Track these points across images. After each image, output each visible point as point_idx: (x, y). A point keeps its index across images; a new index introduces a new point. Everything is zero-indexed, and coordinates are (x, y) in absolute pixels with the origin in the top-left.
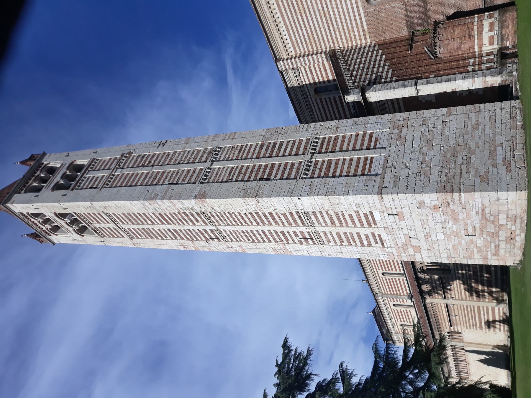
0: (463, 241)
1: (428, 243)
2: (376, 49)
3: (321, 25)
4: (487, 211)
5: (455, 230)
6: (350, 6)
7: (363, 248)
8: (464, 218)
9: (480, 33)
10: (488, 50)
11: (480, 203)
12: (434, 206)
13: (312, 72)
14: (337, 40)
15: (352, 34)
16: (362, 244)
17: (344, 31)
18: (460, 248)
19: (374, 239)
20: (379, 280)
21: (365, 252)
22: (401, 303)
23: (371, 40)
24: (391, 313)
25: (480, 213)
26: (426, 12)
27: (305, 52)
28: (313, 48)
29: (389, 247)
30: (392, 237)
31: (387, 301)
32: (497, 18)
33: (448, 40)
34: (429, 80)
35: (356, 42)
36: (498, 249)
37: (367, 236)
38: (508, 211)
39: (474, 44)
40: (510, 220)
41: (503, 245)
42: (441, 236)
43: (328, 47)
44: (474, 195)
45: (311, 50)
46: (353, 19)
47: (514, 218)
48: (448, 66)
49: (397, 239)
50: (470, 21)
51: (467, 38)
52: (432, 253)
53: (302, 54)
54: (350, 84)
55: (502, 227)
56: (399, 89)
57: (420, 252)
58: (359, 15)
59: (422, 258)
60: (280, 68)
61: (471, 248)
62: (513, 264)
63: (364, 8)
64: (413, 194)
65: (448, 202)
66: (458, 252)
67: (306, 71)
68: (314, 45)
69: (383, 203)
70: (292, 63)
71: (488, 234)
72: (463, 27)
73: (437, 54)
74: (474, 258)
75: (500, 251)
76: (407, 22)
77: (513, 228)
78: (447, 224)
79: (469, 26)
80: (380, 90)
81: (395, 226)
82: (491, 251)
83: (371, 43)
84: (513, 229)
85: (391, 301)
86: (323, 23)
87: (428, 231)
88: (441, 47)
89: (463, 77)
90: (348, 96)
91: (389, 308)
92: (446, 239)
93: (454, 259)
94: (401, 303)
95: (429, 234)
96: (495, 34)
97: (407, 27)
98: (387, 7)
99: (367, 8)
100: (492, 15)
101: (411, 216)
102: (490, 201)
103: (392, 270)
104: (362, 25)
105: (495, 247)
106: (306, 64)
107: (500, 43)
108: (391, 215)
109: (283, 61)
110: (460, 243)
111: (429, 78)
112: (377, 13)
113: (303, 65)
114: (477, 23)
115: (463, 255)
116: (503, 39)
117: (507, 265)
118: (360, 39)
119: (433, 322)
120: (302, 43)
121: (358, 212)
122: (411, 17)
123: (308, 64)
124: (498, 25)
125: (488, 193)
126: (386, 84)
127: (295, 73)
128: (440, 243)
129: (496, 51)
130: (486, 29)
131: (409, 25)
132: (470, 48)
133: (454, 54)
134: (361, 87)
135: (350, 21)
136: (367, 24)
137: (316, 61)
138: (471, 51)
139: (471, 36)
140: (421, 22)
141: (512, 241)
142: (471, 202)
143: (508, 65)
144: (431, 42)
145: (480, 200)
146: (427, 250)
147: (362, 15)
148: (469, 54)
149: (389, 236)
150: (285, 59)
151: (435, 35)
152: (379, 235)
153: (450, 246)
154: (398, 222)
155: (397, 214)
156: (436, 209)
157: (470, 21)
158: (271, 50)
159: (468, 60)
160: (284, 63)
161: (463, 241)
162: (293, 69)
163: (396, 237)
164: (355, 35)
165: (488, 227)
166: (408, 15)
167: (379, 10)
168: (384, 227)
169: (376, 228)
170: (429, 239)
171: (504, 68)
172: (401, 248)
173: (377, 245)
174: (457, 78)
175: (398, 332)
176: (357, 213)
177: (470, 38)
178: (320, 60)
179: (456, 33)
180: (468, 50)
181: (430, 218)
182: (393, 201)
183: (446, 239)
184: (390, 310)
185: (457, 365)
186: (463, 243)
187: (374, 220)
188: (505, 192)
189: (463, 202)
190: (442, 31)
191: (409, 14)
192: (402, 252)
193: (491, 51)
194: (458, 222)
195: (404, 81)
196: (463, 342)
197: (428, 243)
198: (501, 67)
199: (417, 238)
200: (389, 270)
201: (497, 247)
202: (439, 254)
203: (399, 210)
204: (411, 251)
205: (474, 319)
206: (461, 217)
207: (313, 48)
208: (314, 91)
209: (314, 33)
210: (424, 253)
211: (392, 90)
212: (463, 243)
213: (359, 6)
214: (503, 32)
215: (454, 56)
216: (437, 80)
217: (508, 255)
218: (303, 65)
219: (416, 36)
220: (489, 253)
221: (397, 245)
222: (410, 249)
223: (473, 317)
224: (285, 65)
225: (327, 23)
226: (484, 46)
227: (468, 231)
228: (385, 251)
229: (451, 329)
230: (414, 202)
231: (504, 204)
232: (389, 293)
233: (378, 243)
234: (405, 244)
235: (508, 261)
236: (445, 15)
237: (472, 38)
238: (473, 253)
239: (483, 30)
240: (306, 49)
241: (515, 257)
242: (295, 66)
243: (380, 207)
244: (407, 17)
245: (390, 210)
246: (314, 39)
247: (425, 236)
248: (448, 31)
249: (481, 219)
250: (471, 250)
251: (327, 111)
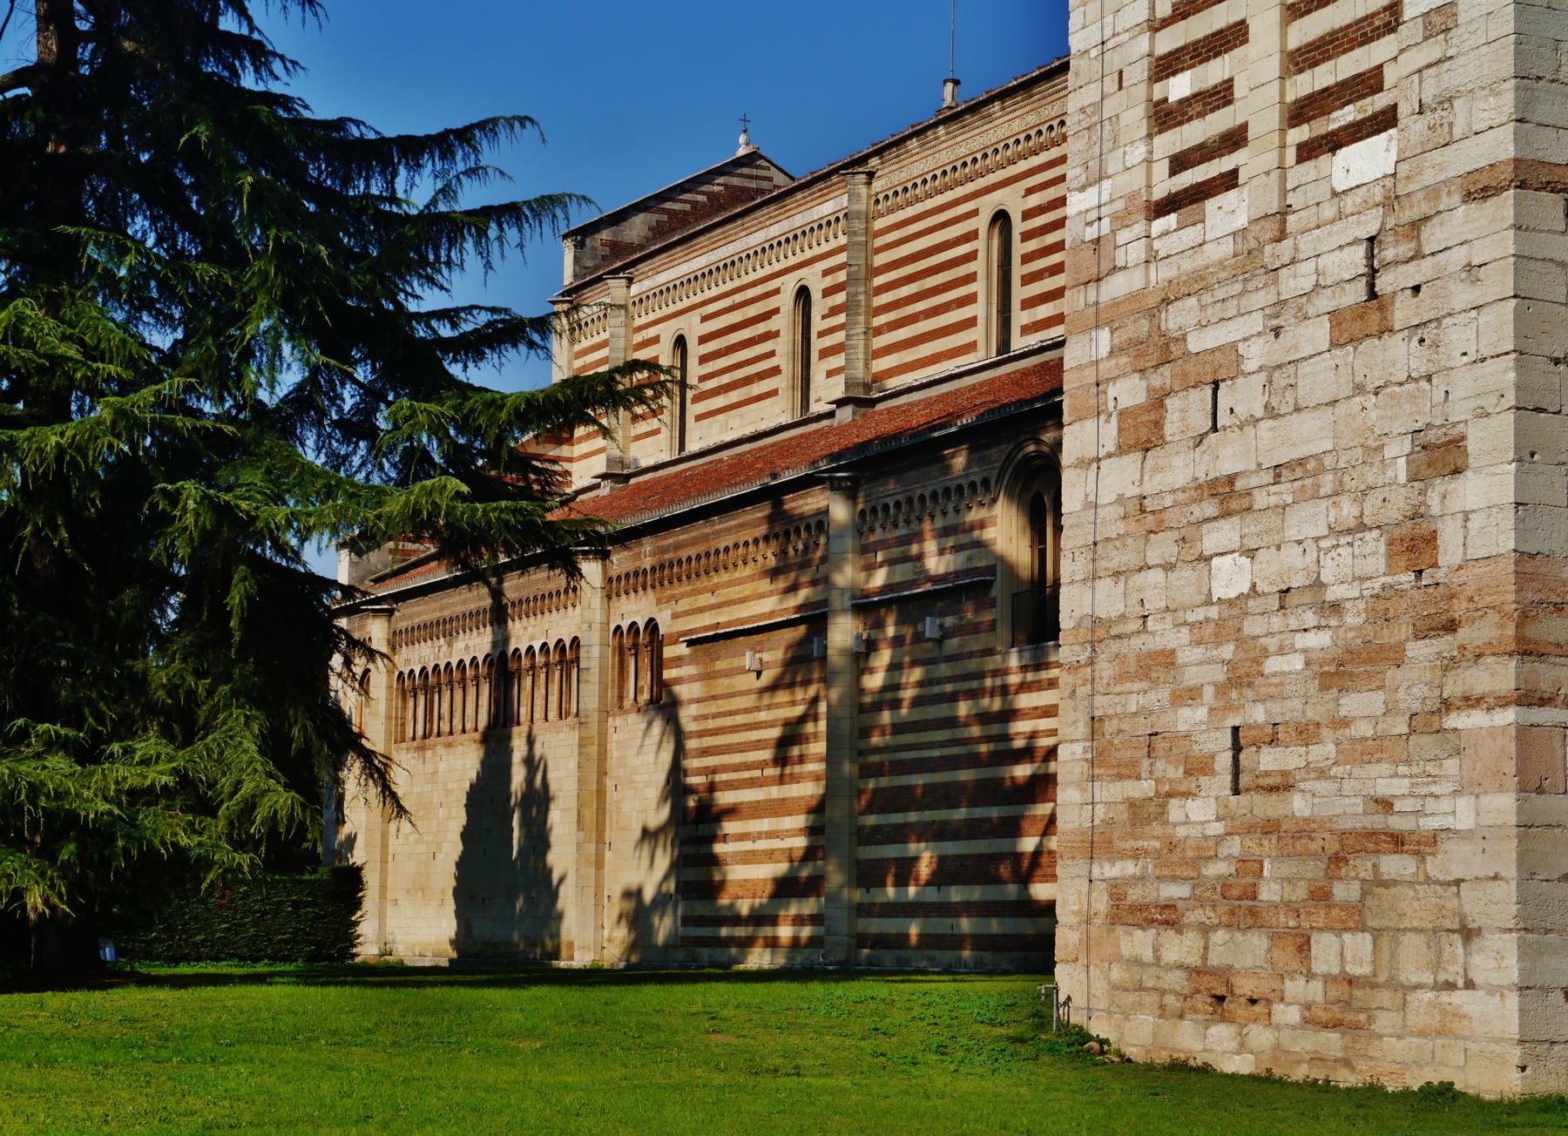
0: (1201, 713)
1: (1181, 496)
4: (1395, 865)
5: (1272, 665)
7: (1138, 73)
8: (1345, 723)
11: (1449, 822)
12: (1431, 539)
16: (1166, 67)
18: (1152, 696)
19: (1202, 146)
20: (960, 192)
21: (1111, 84)
22: (821, 334)
24: (753, 277)
25: (1378, 821)
29: (1150, 248)
30: (1221, 264)
31: (825, 248)
36: (1151, 921)
37: (1222, 95)
38: (1394, 984)
40: (1333, 994)
41: (1180, 948)
42: (1230, 577)
44: (1501, 789)
47: (1350, 1017)
49: (1207, 298)
52: (1121, 527)
55: (1291, 949)
57: (1122, 450)
59: (1083, 464)
61: (1160, 765)
62: (1062, 998)
64: (1511, 399)
65: (1451, 627)
66: (1127, 686)
69: (1457, 198)
71: (1250, 867)
74: (1093, 779)
75: (1139, 933)
77: (1288, 1014)
78: (1310, 619)
81: (1295, 282)
82: (1142, 878)
84: (1278, 1008)
85: (826, 273)
87: (1261, 500)
91: (784, 264)
92: (1213, 612)
93: (1083, 657)
94: (821, 334)
95: (1245, 503)
101: (1359, 389)
102: (1458, 882)
103: (1028, 279)
105: (1170, 906)
108: (1370, 256)
110: (1192, 695)
115: (1111, 712)
117: (1060, 971)
119: (705, 538)
121: (1391, 28)
125: (1510, 871)
128: (1185, 574)
141: (1202, 1002)
142: (1451, 766)
145: (1465, 821)
146: (1137, 491)
149: (1227, 248)
152: (1229, 180)
153: (1165, 636)
154: (1324, 303)
155: (1372, 295)
156: (1411, 549)
161: (1201, 713)
163: (1220, 293)
165: (1287, 869)
168: (1285, 212)
169: (1282, 157)
170: (1210, 508)
172: (1144, 326)
173: (1161, 168)
175: (638, 322)
176: (1386, 17)
181: (1348, 510)
182: (1469, 267)
183: (1213, 612)
184: (768, 270)
185: (469, 673)
186: (1191, 717)
187: (1333, 143)
188: (1514, 976)
189: (1454, 720)
192: (1122, 336)
194: (1324, 688)
196: (605, 713)
197: (1181, 496)
199: (1215, 429)
200: (1027, 259)
201: (1167, 917)
202: (1114, 565)
203: (1404, 311)
204: (1129, 392)
205: (747, 774)
206: (1353, 704)
210: (1122, 476)
212: (1191, 717)
217: (1116, 974)
220: (1129, 868)
221: (1167, 302)
222: (1144, 383)
223: (757, 773)
227: (1266, 749)
228: (1121, 221)
229: (676, 642)
230: (1459, 411)
231: (1436, 966)
232: (880, 260)
234: (1175, 350)
235: (1083, 976)
238: (1128, 772)
241: (1110, 1013)
243: (1429, 178)
245: (1405, 249)
247: (1231, 479)
249: (1347, 824)
250: (1146, 763)
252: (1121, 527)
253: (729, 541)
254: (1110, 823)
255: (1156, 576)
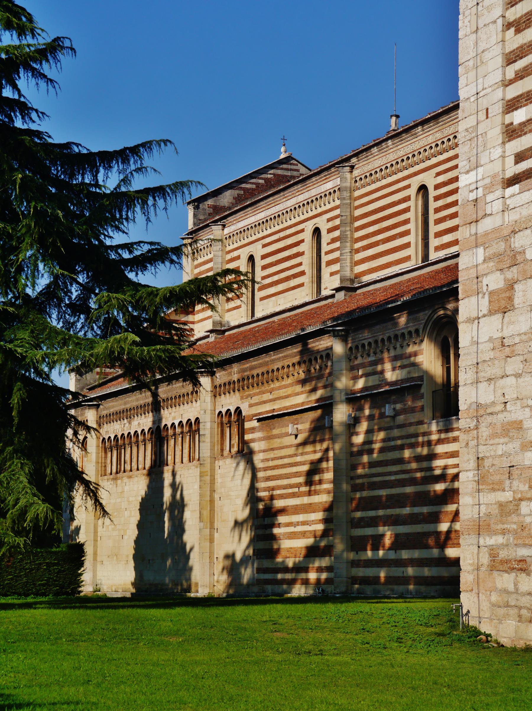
1: (524, 337)
7: (497, 109)
18: (510, 446)
20: (400, 175)
22: (327, 253)
24: (290, 223)
31: (328, 207)
36: (514, 569)
52: (492, 354)
57: (491, 313)
59: (470, 321)
61: (515, 483)
62: (465, 611)
66: (497, 440)
74: (479, 491)
75: (506, 575)
82: (507, 545)
85: (329, 220)
91: (306, 216)
94: (327, 253)
103: (438, 222)
105: (522, 561)
115: (488, 454)
117: (462, 596)
119: (266, 364)
146: (500, 335)
172: (502, 246)
173: (510, 160)
175: (228, 248)
184: (298, 219)
185: (141, 438)
192: (490, 251)
196: (214, 459)
197: (524, 337)
200: (437, 210)
202: (488, 375)
205: (290, 491)
217: (494, 598)
220: (499, 540)
221: (514, 232)
222: (503, 276)
223: (296, 490)
228: (489, 189)
229: (251, 420)
232: (358, 213)
233: (517, 162)
235: (476, 599)
238: (497, 487)
241: (491, 620)
250: (507, 482)
252: (492, 354)
253: (279, 365)
254: (489, 515)
255: (511, 381)
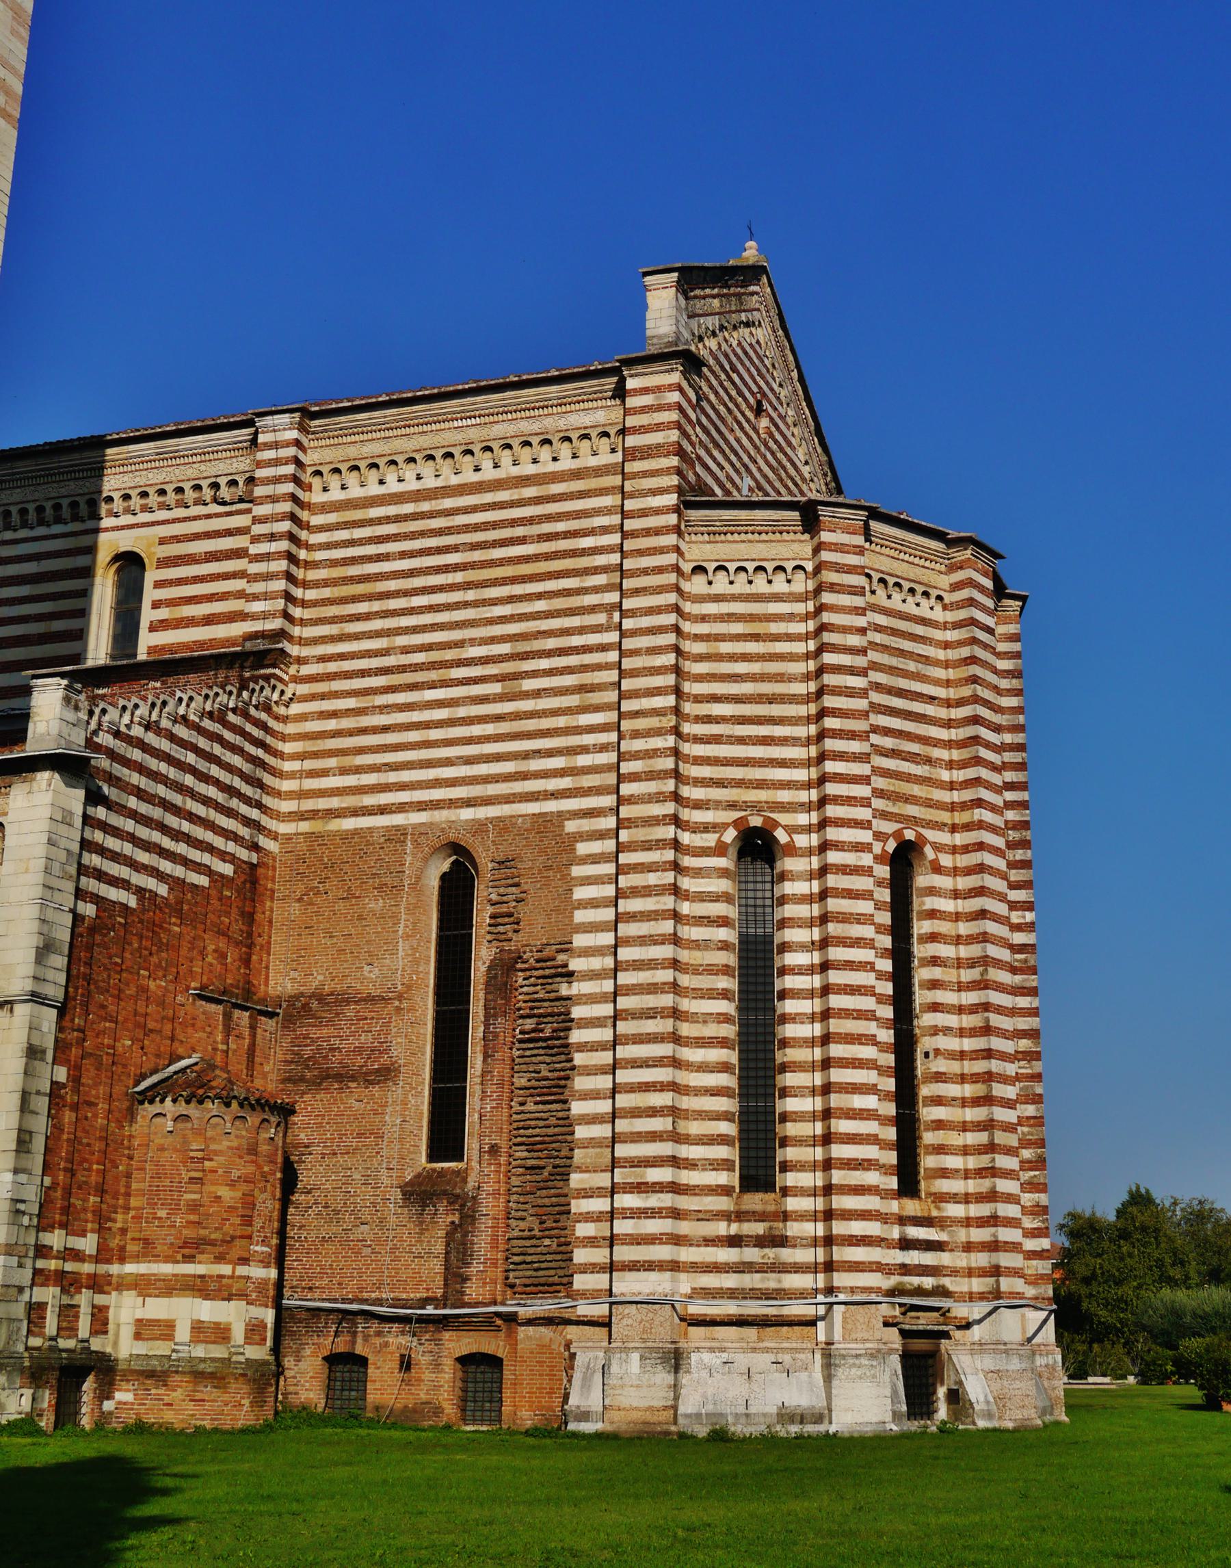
2: (243, 854)
3: (401, 641)
6: (444, 776)
9: (202, 1288)
10: (117, 1316)
13: (218, 560)
14: (323, 697)
15: (332, 762)
17: (351, 733)
23: (288, 838)
26: (339, 1077)
27: (309, 547)
28: (317, 584)
32: (243, 1354)
33: (200, 1155)
34: (43, 1060)
35: (292, 775)
39: (156, 1258)
43: (305, 652)
45: (312, 575)
46: (393, 777)
48: (89, 1145)
50: (258, 1248)
51: (188, 1233)
53: (303, 535)
54: (113, 714)
56: (35, 926)
58: (402, 808)
60: (269, 420)
63: (420, 832)
67: (229, 533)
68: (327, 593)
70: (277, 480)
72: (238, 1221)
73: (151, 1102)
76: (320, 997)
79: (237, 1242)
80: (51, 843)
83: (275, 836)
86: (406, 650)
88: (180, 1125)
89: (22, 1207)
90: (60, 694)
96: (176, 1344)
97: (302, 994)
98: (402, 926)
99: (417, 844)
100: (257, 1337)
104: (356, 812)
106: (256, 539)
107: (135, 1366)
109: (298, 443)
111: (55, 1061)
112: (388, 880)
113: (258, 529)
114: (240, 1277)
116: (148, 1377)
118: (301, 795)
120: (352, 543)
122: (338, 1014)
123: (254, 550)
124: (213, 1360)
126: (73, 870)
127: (233, 483)
129: (103, 1346)
130: (208, 1310)
131: (305, 1006)
132: (146, 1242)
133: (135, 1174)
134: (89, 759)
135: (386, 765)
136: (356, 832)
137: (258, 587)
138: (132, 1248)
139: (190, 1249)
140: (307, 1052)
143: (28, 1392)
144: (214, 1084)
147: (398, 819)
148: (118, 1237)
150: (301, 456)
151: (234, 1104)
157: (258, 1248)
158: (357, 403)
159: (93, 1231)
160: (287, 444)
162: (251, 481)
164: (324, 773)
166: (348, 1002)
167: (398, 888)
171: (18, 1381)
174: (23, 1178)
177: (186, 1245)
178: (257, 607)
179: (225, 1192)
180: (137, 1235)
190: (244, 1133)
191: (350, 1011)
193: (111, 1327)
195: (66, 951)
198: (27, 1364)
207: (317, 584)
208: (129, 549)
209: (376, 606)
211: (38, 891)
213: (436, 813)
214: (178, 1378)
215: (128, 1175)
216: (38, 1093)
218: (258, 529)
219: (253, 1028)
224: (276, 445)
225: (402, 669)
226: (141, 1299)
236: (310, 1154)
237: (187, 1251)
239: (207, 1297)
240: (320, 555)
242: (259, 491)
244: (344, 999)
246: (355, 599)
248: (241, 1157)
251: (24, 591)
